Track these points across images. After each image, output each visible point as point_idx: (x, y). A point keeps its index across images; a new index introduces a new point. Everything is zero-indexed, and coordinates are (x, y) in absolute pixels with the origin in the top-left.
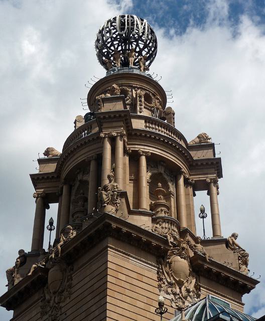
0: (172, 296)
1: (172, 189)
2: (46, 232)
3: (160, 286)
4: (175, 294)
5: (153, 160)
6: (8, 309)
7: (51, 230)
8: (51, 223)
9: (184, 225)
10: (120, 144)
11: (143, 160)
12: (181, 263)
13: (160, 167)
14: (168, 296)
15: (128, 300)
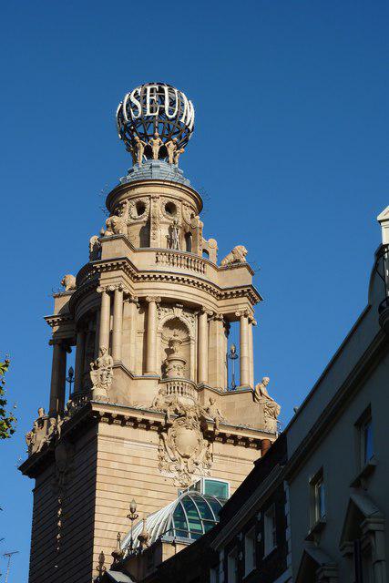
0: (176, 474)
1: (193, 334)
2: (67, 384)
3: (161, 466)
4: (179, 471)
5: (167, 303)
6: (31, 477)
7: (70, 382)
8: (71, 375)
9: (204, 378)
10: (119, 296)
11: (153, 307)
12: (189, 435)
13: (176, 309)
14: (170, 475)
15: (122, 489)
